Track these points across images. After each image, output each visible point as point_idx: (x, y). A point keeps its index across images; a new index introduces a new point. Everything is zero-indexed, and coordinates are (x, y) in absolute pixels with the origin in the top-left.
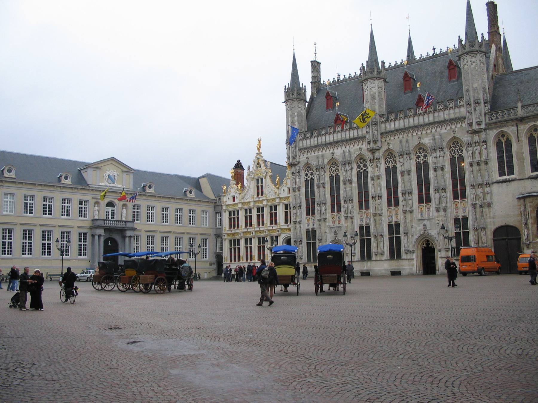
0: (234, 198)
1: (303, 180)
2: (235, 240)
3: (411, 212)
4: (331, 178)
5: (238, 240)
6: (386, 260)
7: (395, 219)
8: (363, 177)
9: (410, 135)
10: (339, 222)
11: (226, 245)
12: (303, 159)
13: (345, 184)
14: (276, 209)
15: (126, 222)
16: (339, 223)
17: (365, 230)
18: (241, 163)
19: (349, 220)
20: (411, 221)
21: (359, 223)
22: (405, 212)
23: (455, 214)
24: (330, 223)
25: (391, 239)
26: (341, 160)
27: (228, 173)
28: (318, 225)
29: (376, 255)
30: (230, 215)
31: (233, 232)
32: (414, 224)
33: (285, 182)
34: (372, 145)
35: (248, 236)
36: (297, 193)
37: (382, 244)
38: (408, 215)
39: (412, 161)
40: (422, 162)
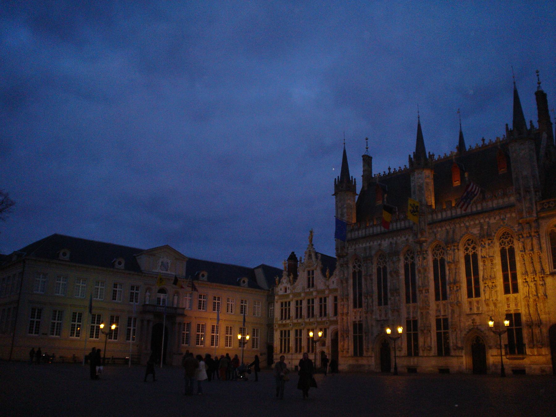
0: (286, 289)
1: (351, 271)
2: (285, 331)
4: (379, 270)
5: (289, 331)
6: (433, 356)
7: (442, 313)
8: (410, 270)
10: (386, 314)
11: (277, 335)
12: (351, 250)
14: (325, 301)
15: (176, 308)
16: (386, 316)
23: (506, 308)
25: (439, 335)
27: (281, 265)
29: (423, 351)
30: (282, 306)
31: (284, 322)
33: (334, 273)
35: (298, 328)
37: (429, 339)
39: (460, 252)
40: (471, 254)
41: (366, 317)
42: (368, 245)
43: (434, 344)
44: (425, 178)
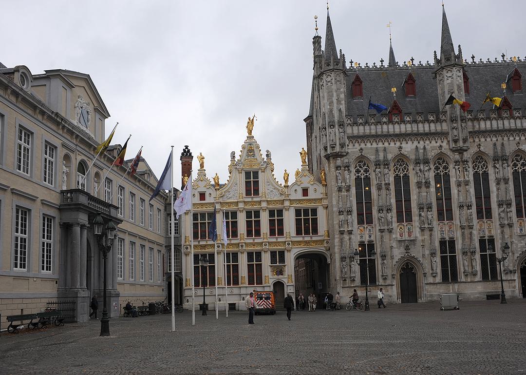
3: (510, 226)
7: (487, 234)
9: (506, 138)
13: (419, 187)
17: (447, 246)
18: (189, 151)
19: (427, 233)
20: (511, 236)
21: (440, 236)
22: (502, 226)
24: (396, 235)
26: (413, 157)
28: (378, 237)
29: (466, 275)
32: (514, 240)
34: (461, 144)
36: (344, 193)
38: (507, 230)
41: (382, 237)
42: (380, 145)
43: (478, 268)
44: (452, 80)
